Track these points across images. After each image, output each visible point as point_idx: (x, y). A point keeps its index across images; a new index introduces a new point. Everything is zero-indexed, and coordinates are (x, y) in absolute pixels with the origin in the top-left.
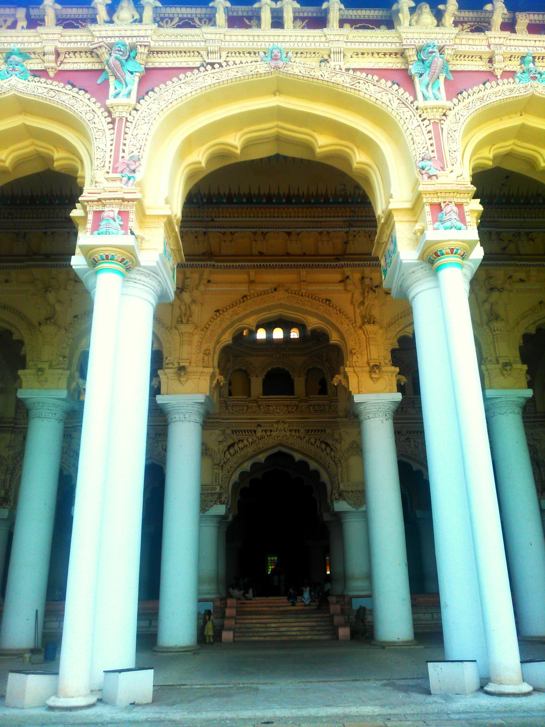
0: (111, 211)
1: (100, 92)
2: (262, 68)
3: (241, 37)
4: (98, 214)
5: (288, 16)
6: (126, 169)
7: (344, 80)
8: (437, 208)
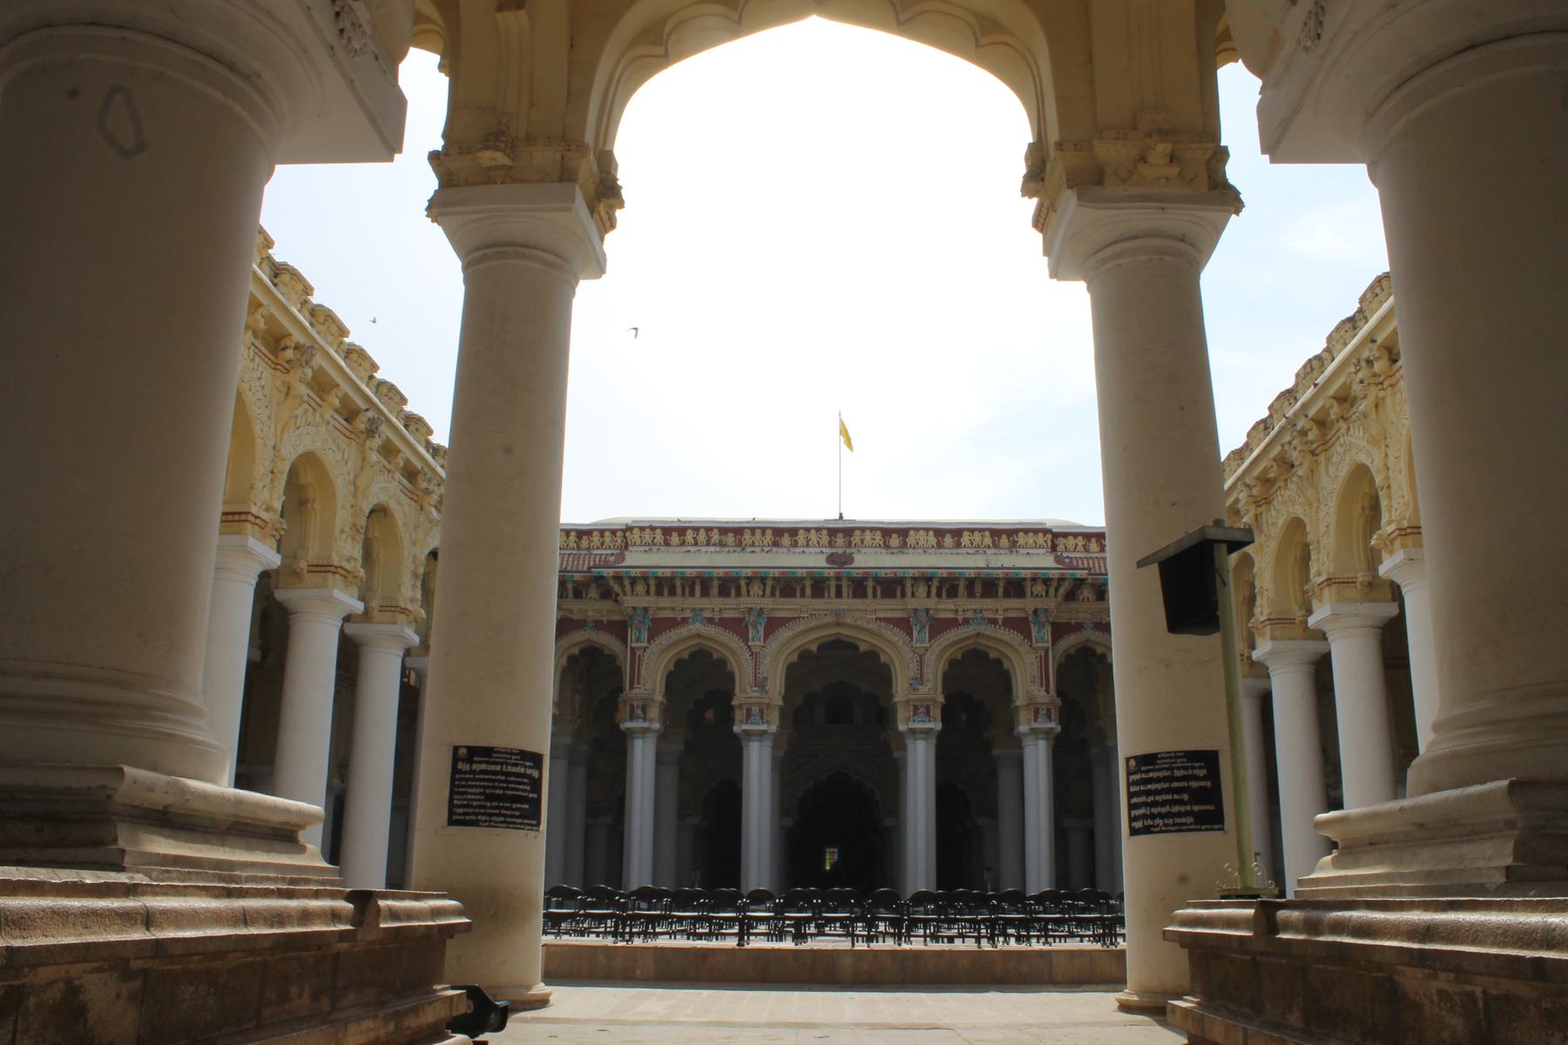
0: (755, 710)
1: (746, 640)
2: (829, 619)
3: (818, 603)
4: (749, 712)
5: (845, 590)
6: (761, 684)
7: (873, 626)
8: (916, 708)
